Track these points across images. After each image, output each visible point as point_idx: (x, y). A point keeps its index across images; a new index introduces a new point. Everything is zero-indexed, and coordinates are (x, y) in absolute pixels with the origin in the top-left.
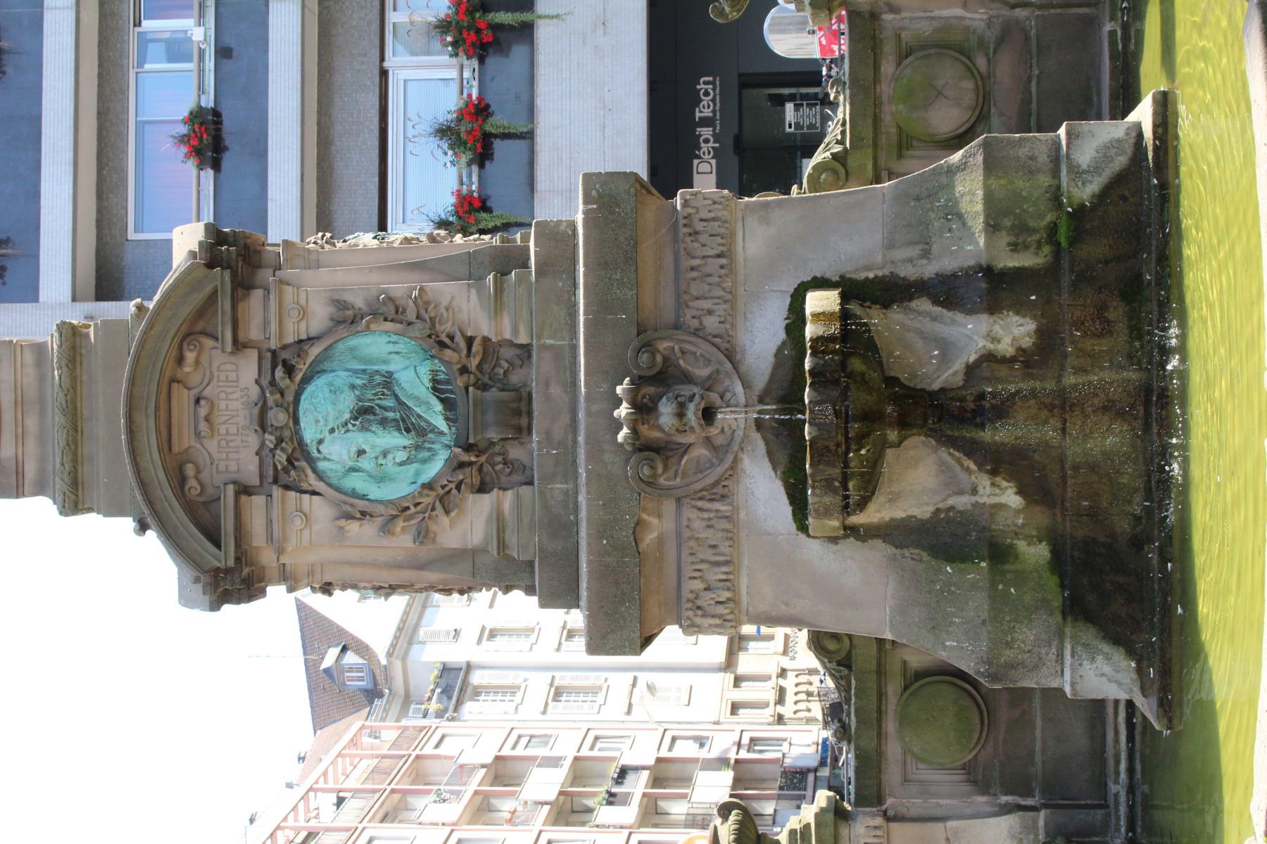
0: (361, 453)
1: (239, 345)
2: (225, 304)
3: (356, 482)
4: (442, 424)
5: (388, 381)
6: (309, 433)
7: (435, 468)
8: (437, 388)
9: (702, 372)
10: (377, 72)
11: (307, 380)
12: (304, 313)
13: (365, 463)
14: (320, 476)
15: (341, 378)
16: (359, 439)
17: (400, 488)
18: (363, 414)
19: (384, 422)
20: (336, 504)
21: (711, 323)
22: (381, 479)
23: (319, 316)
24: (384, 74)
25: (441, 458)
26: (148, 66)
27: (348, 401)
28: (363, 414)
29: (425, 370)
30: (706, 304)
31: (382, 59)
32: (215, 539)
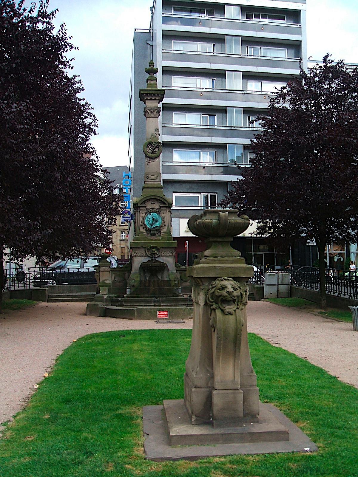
0: (150, 219)
1: (161, 207)
2: (165, 205)
3: (147, 218)
4: (152, 227)
5: (157, 222)
6: (151, 214)
7: (148, 227)
8: (156, 227)
9: (158, 254)
10: (200, 192)
11: (157, 213)
12: (164, 213)
13: (149, 219)
14: (147, 215)
15: (157, 217)
16: (151, 219)
17: (146, 222)
18: (153, 219)
19: (153, 221)
20: (144, 216)
21: (162, 254)
22: (147, 221)
23: (163, 215)
24: (200, 193)
25: (149, 227)
26: (202, 152)
27: (155, 218)
28: (153, 219)
29: (158, 225)
30: (164, 253)
31: (202, 193)
32: (141, 204)
